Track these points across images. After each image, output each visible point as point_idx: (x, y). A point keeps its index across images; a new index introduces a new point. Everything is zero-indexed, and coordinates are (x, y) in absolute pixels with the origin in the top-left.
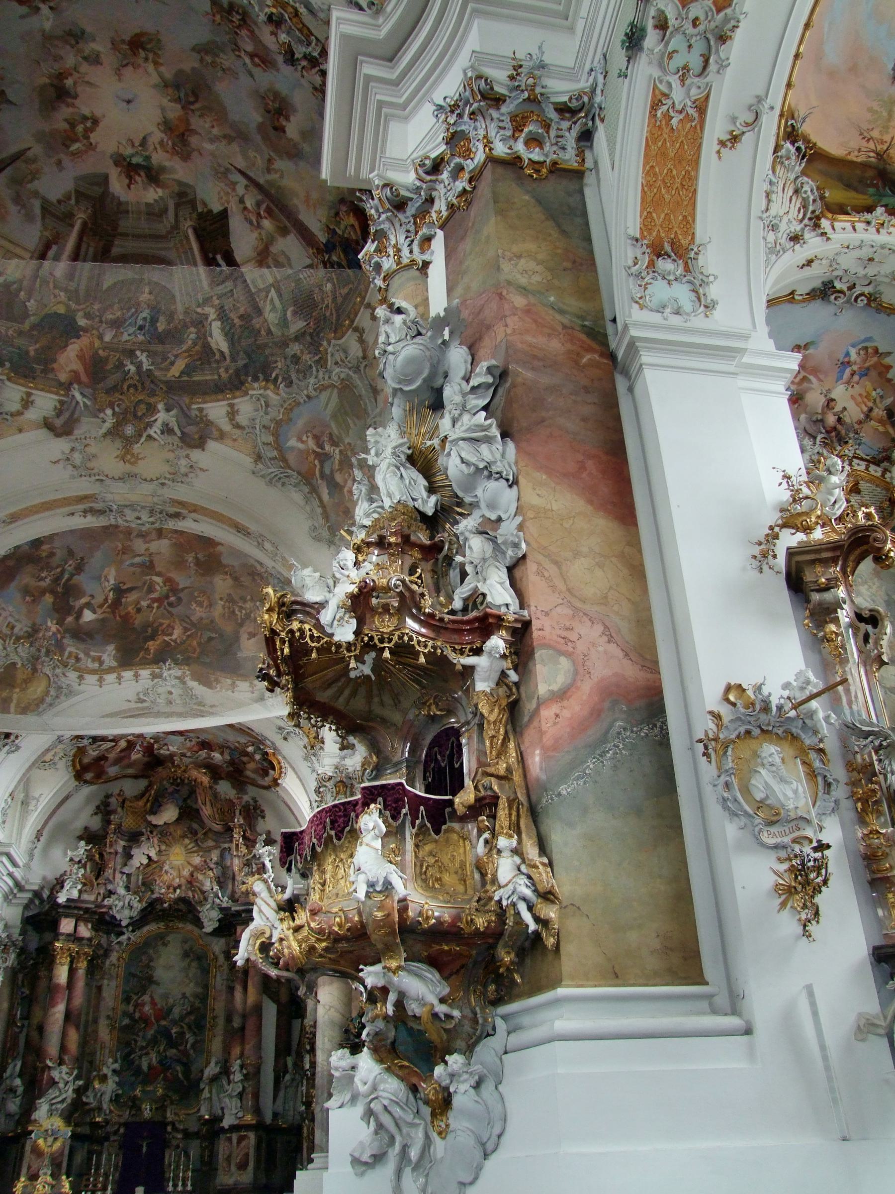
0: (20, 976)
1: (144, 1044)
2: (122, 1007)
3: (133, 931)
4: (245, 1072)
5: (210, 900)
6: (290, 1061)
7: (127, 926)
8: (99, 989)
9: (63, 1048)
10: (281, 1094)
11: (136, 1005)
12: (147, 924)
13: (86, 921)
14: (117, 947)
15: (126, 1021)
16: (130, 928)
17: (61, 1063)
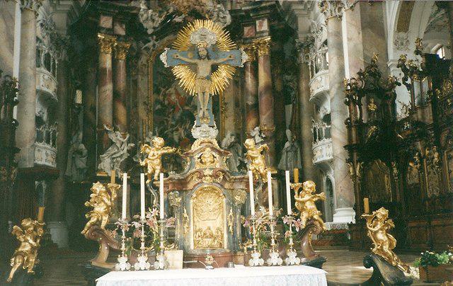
0: (72, 71)
1: (174, 123)
2: (153, 97)
3: (157, 40)
4: (264, 136)
5: (215, 14)
6: (288, 132)
7: (152, 35)
8: (135, 82)
9: (115, 120)
10: (284, 157)
11: (165, 95)
12: (167, 35)
13: (121, 23)
14: (145, 52)
15: (159, 107)
16: (155, 37)
17: (116, 130)
